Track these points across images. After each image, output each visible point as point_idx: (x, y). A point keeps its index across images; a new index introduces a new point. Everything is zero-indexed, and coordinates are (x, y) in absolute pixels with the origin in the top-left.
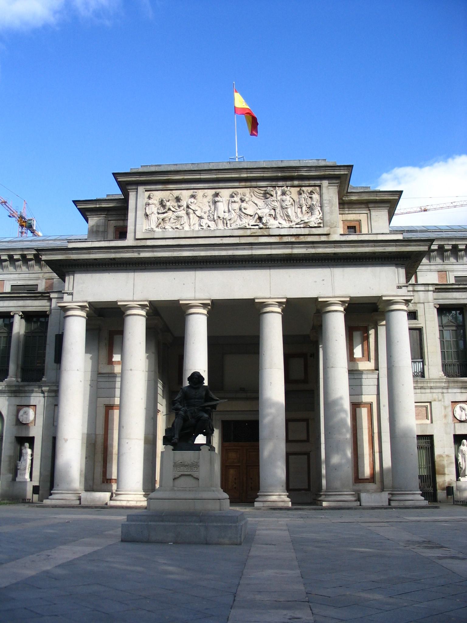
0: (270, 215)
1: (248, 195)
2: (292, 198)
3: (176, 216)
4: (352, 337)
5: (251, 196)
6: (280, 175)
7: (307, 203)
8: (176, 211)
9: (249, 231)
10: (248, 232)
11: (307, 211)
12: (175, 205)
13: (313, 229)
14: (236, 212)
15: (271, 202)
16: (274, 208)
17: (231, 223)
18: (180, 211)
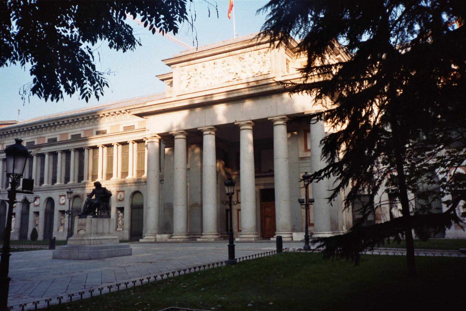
0: (242, 71)
4: (307, 136)
9: (231, 82)
10: (231, 84)
13: (266, 76)
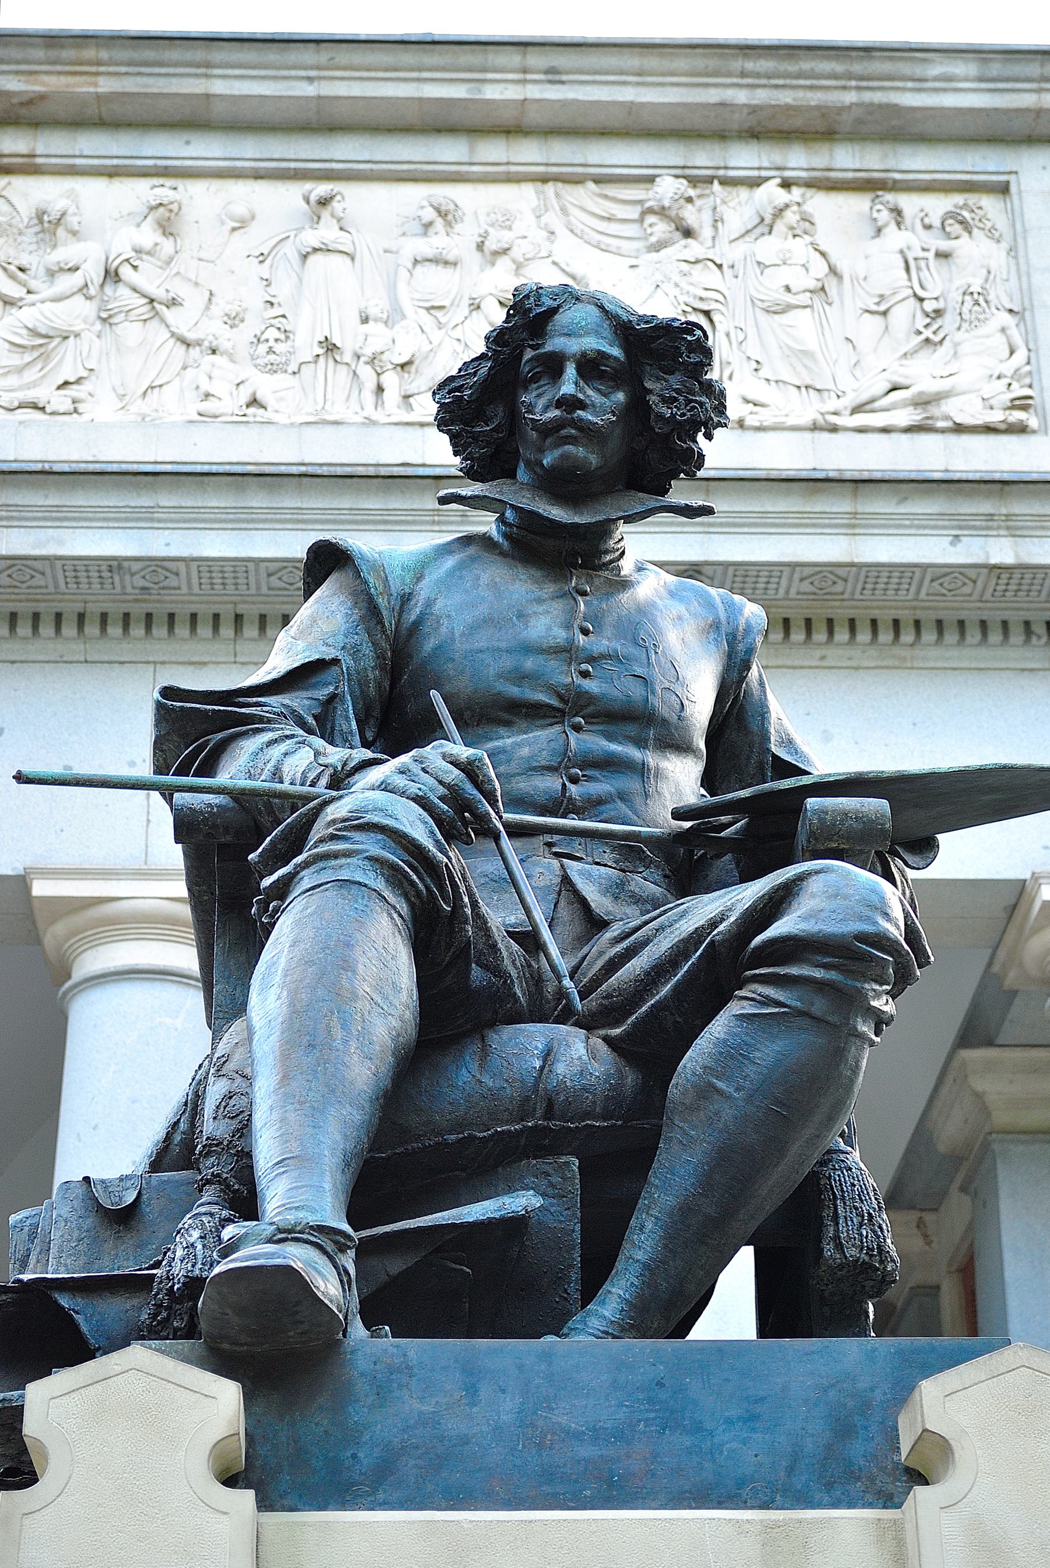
1: (526, 223)
2: (823, 254)
3: (34, 333)
5: (545, 234)
6: (742, 97)
7: (922, 287)
8: (31, 298)
11: (928, 333)
12: (24, 262)
14: (443, 320)
15: (685, 267)
16: (706, 308)
17: (412, 389)
18: (57, 299)
